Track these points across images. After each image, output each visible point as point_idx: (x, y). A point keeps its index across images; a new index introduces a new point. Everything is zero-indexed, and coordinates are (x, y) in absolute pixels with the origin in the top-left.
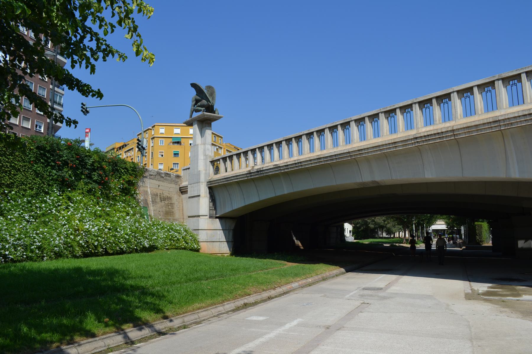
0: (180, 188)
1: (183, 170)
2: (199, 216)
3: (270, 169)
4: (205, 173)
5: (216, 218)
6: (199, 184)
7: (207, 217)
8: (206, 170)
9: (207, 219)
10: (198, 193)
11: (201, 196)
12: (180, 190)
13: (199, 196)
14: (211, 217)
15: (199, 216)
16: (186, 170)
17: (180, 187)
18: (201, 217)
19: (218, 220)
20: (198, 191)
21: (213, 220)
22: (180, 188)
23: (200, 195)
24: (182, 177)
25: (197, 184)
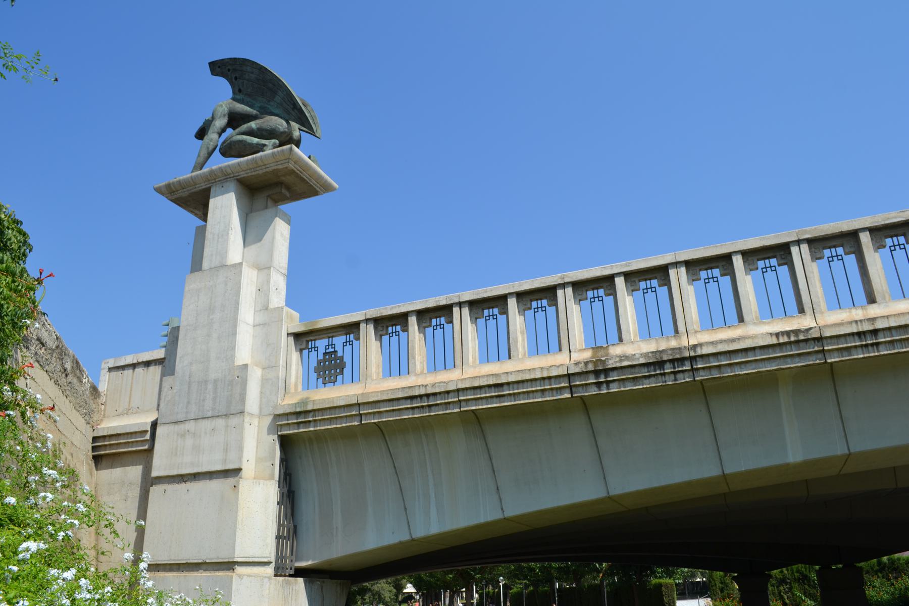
0: (95, 439)
1: (110, 369)
2: (230, 566)
3: (746, 351)
4: (264, 381)
5: (299, 573)
6: (234, 421)
7: (270, 570)
8: (269, 367)
9: (269, 578)
10: (225, 461)
11: (244, 473)
12: (94, 449)
13: (237, 472)
14: (279, 572)
15: (230, 566)
16: (119, 373)
17: (96, 434)
18: (239, 570)
19: (300, 580)
20: (226, 450)
21: (288, 583)
22: (95, 439)
23: (237, 472)
24: (103, 399)
25: (220, 422)
